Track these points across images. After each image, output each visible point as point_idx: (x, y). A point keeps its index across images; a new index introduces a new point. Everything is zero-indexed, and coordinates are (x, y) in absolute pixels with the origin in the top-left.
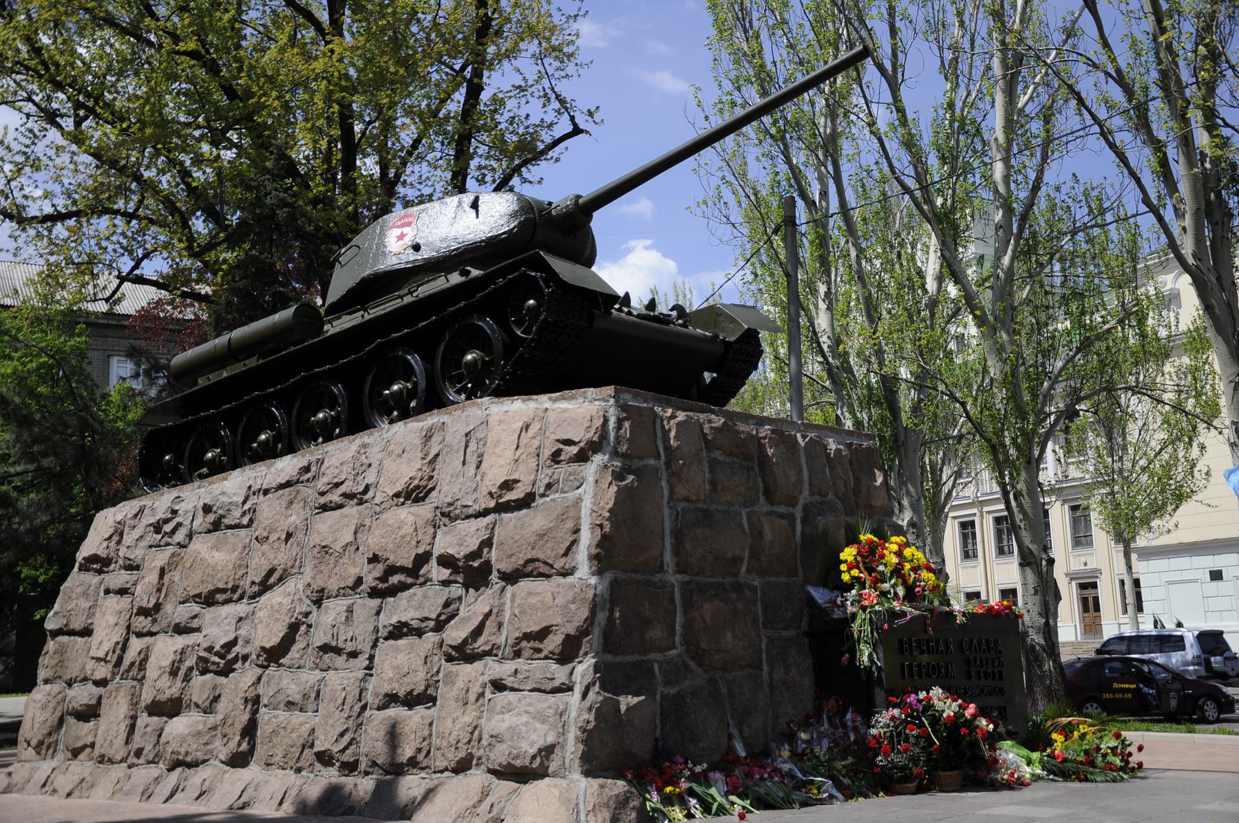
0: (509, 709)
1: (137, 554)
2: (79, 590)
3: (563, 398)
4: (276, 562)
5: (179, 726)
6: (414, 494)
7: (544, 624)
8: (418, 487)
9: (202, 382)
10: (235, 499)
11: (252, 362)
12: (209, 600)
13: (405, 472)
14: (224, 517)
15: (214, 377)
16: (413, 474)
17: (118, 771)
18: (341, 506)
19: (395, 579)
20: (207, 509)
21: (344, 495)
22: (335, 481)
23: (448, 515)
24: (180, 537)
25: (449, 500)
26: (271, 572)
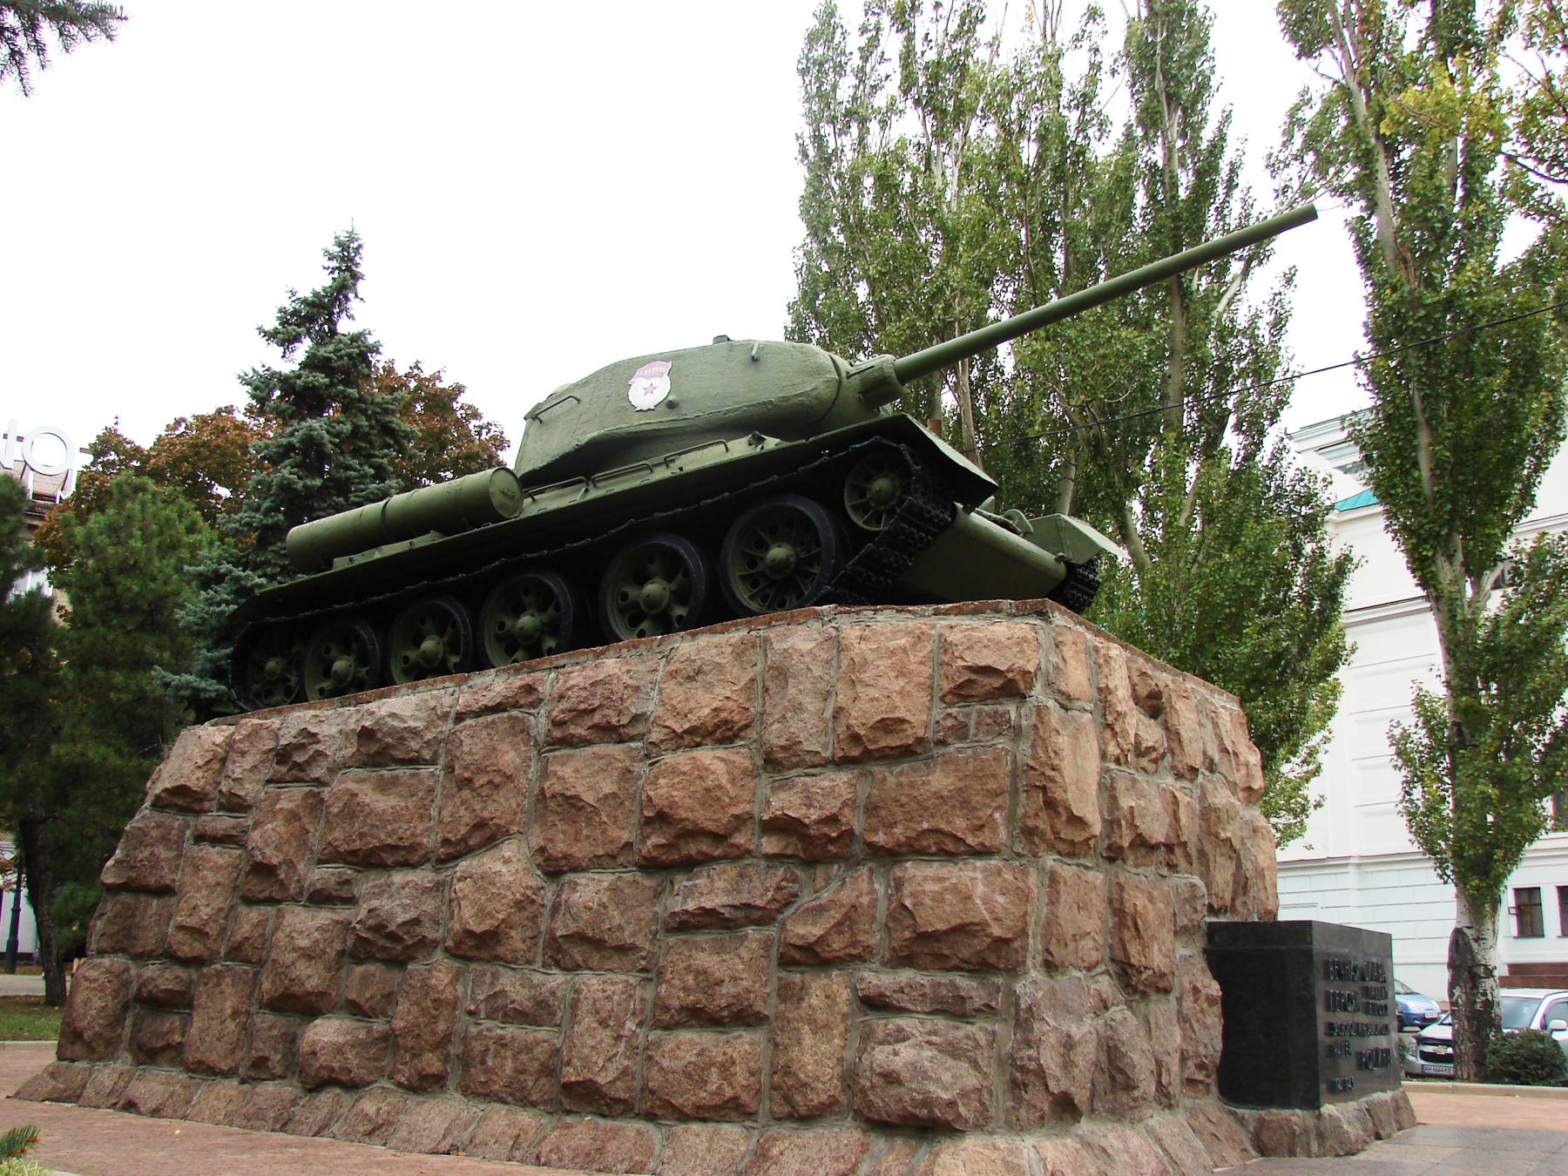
0: (901, 1036)
1: (250, 789)
2: (155, 833)
3: (960, 612)
4: (486, 814)
5: (327, 1032)
6: (723, 732)
7: (955, 922)
8: (726, 722)
9: (341, 564)
10: (412, 724)
11: (421, 541)
12: (370, 860)
13: (704, 704)
14: (393, 746)
15: (360, 559)
16: (716, 704)
17: (230, 1087)
18: (589, 743)
19: (692, 849)
20: (366, 735)
21: (594, 727)
22: (582, 706)
23: (774, 763)
24: (318, 772)
25: (782, 742)
26: (481, 825)
